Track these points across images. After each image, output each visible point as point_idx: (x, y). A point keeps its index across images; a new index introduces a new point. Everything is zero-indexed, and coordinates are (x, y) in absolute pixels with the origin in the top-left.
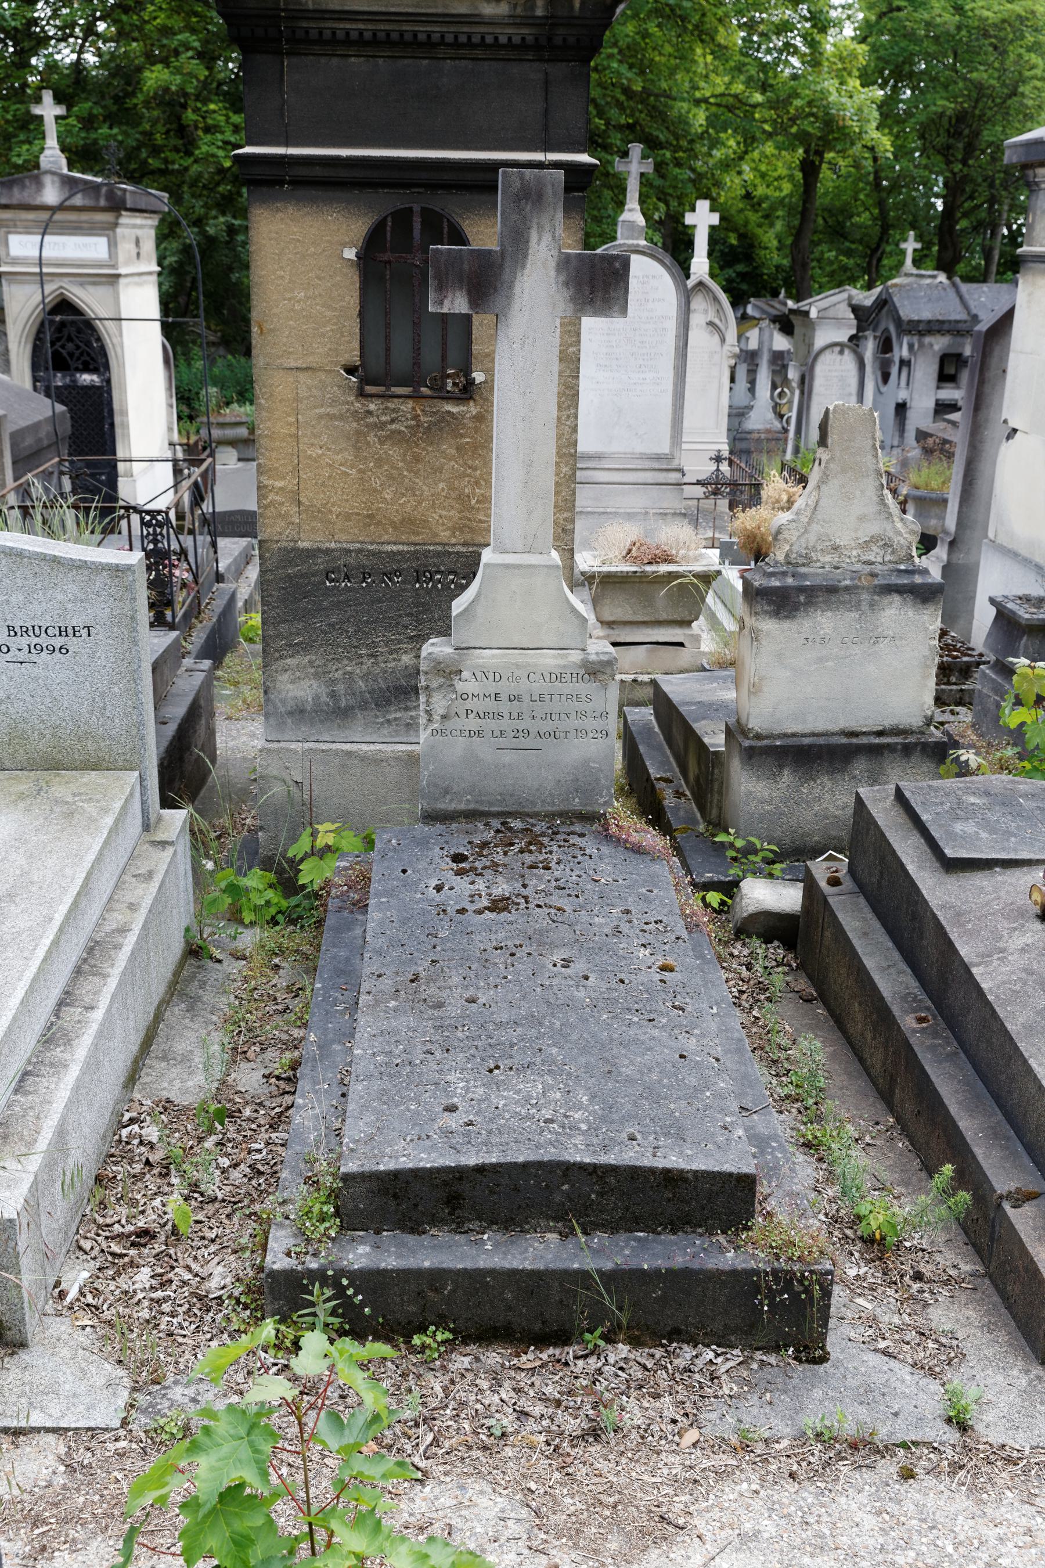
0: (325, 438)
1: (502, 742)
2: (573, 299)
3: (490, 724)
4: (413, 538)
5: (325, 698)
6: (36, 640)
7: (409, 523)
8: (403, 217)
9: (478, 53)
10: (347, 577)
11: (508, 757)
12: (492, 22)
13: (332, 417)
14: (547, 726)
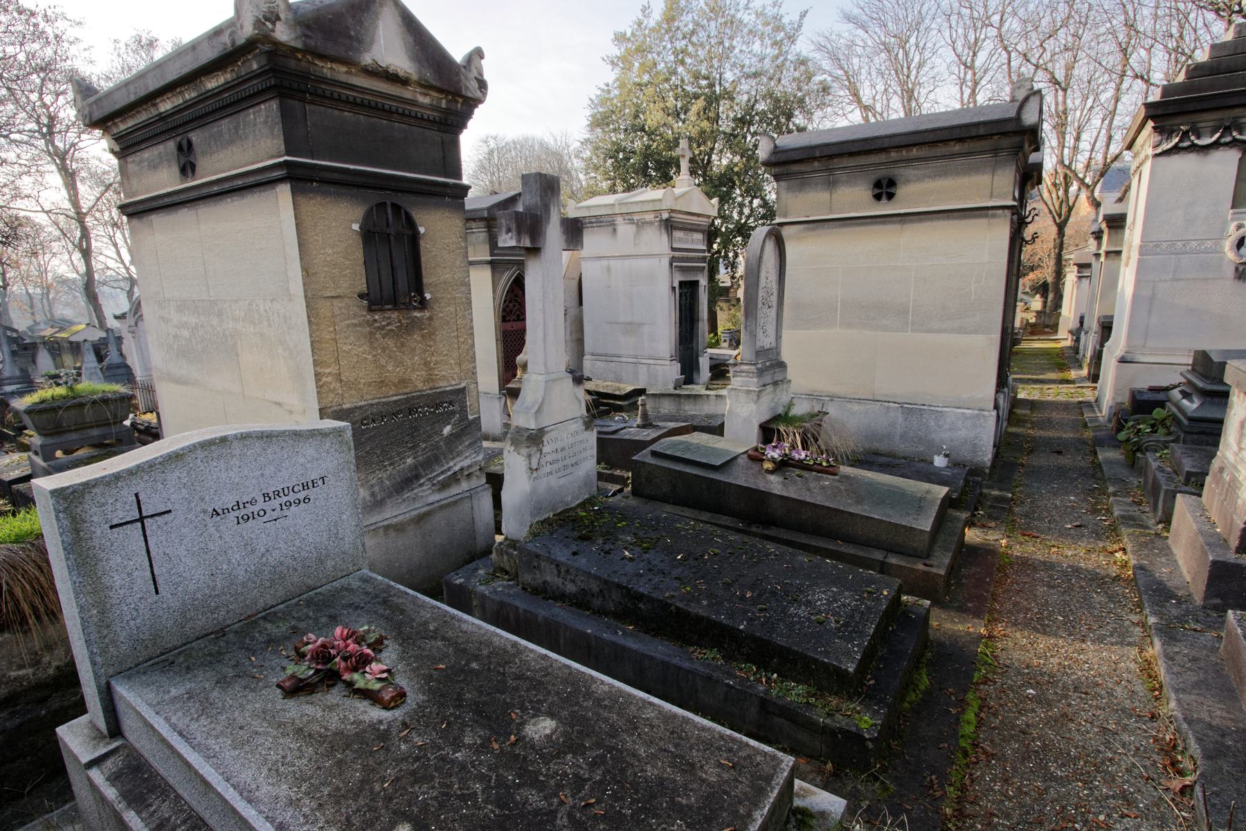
0: (352, 338)
1: (560, 474)
2: (566, 241)
3: (556, 466)
4: (407, 390)
5: (368, 498)
6: (286, 499)
7: (403, 382)
8: (381, 206)
9: (412, 121)
10: (373, 421)
11: (562, 481)
12: (422, 106)
13: (355, 325)
14: (573, 460)
